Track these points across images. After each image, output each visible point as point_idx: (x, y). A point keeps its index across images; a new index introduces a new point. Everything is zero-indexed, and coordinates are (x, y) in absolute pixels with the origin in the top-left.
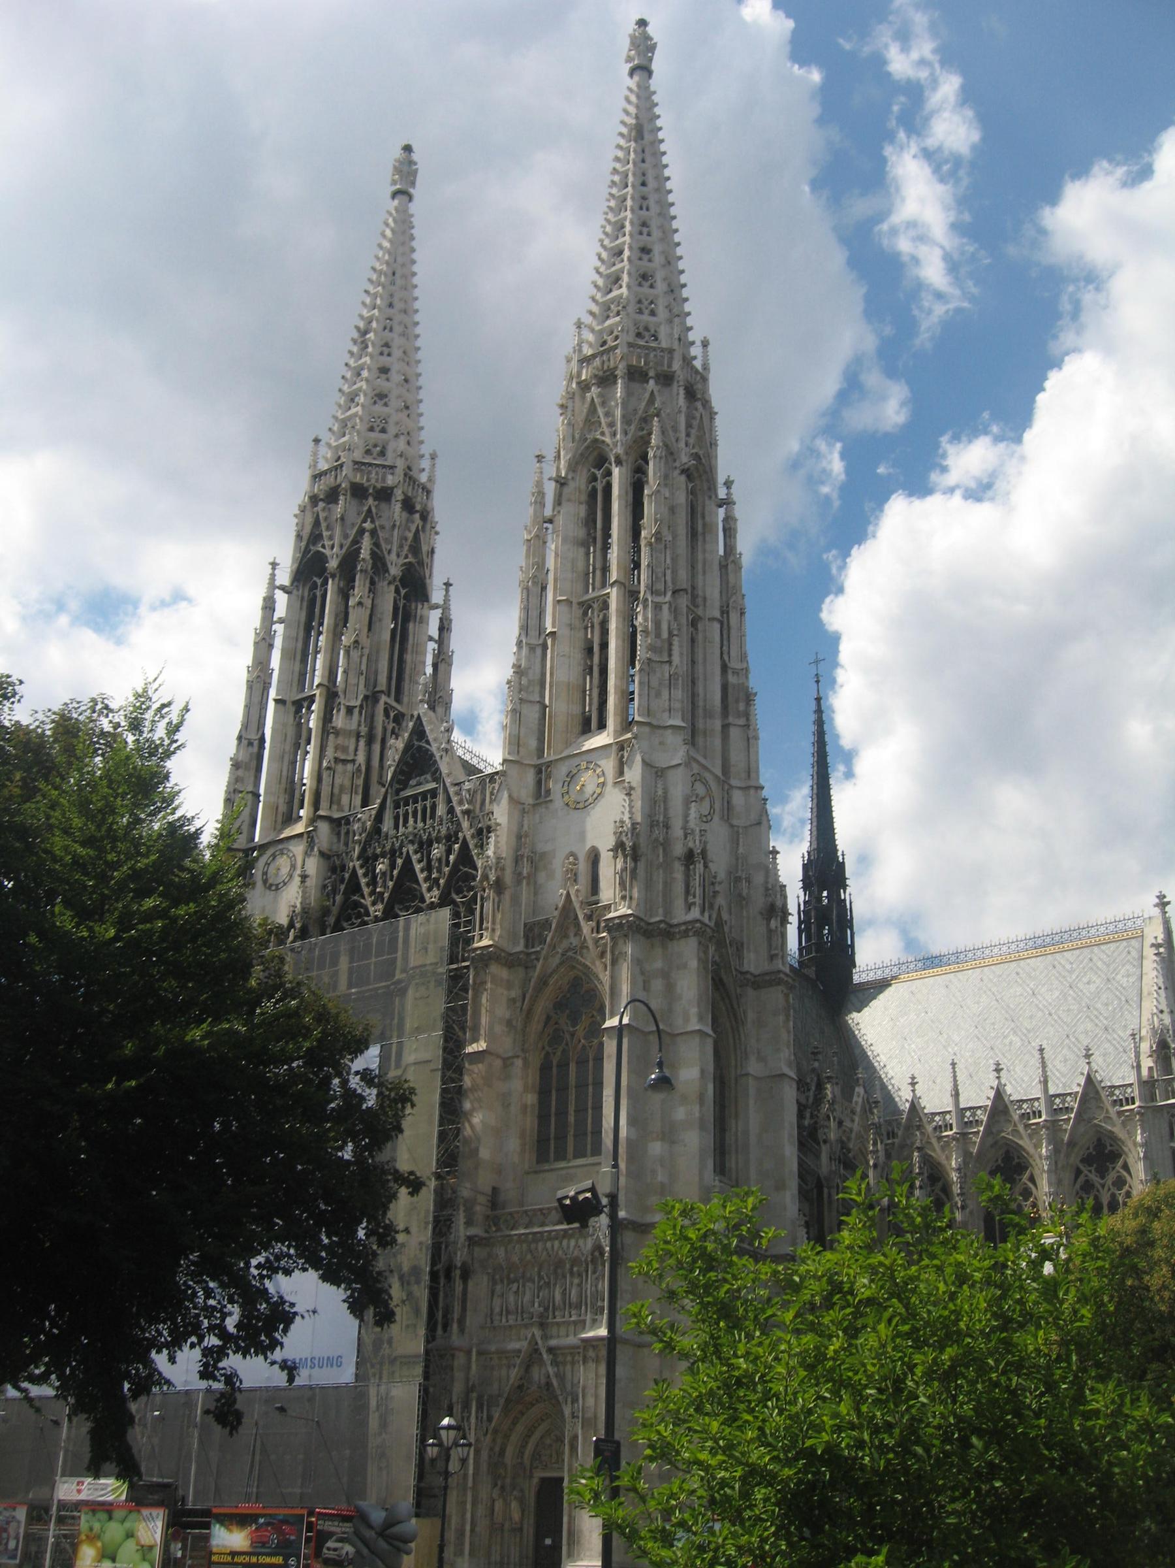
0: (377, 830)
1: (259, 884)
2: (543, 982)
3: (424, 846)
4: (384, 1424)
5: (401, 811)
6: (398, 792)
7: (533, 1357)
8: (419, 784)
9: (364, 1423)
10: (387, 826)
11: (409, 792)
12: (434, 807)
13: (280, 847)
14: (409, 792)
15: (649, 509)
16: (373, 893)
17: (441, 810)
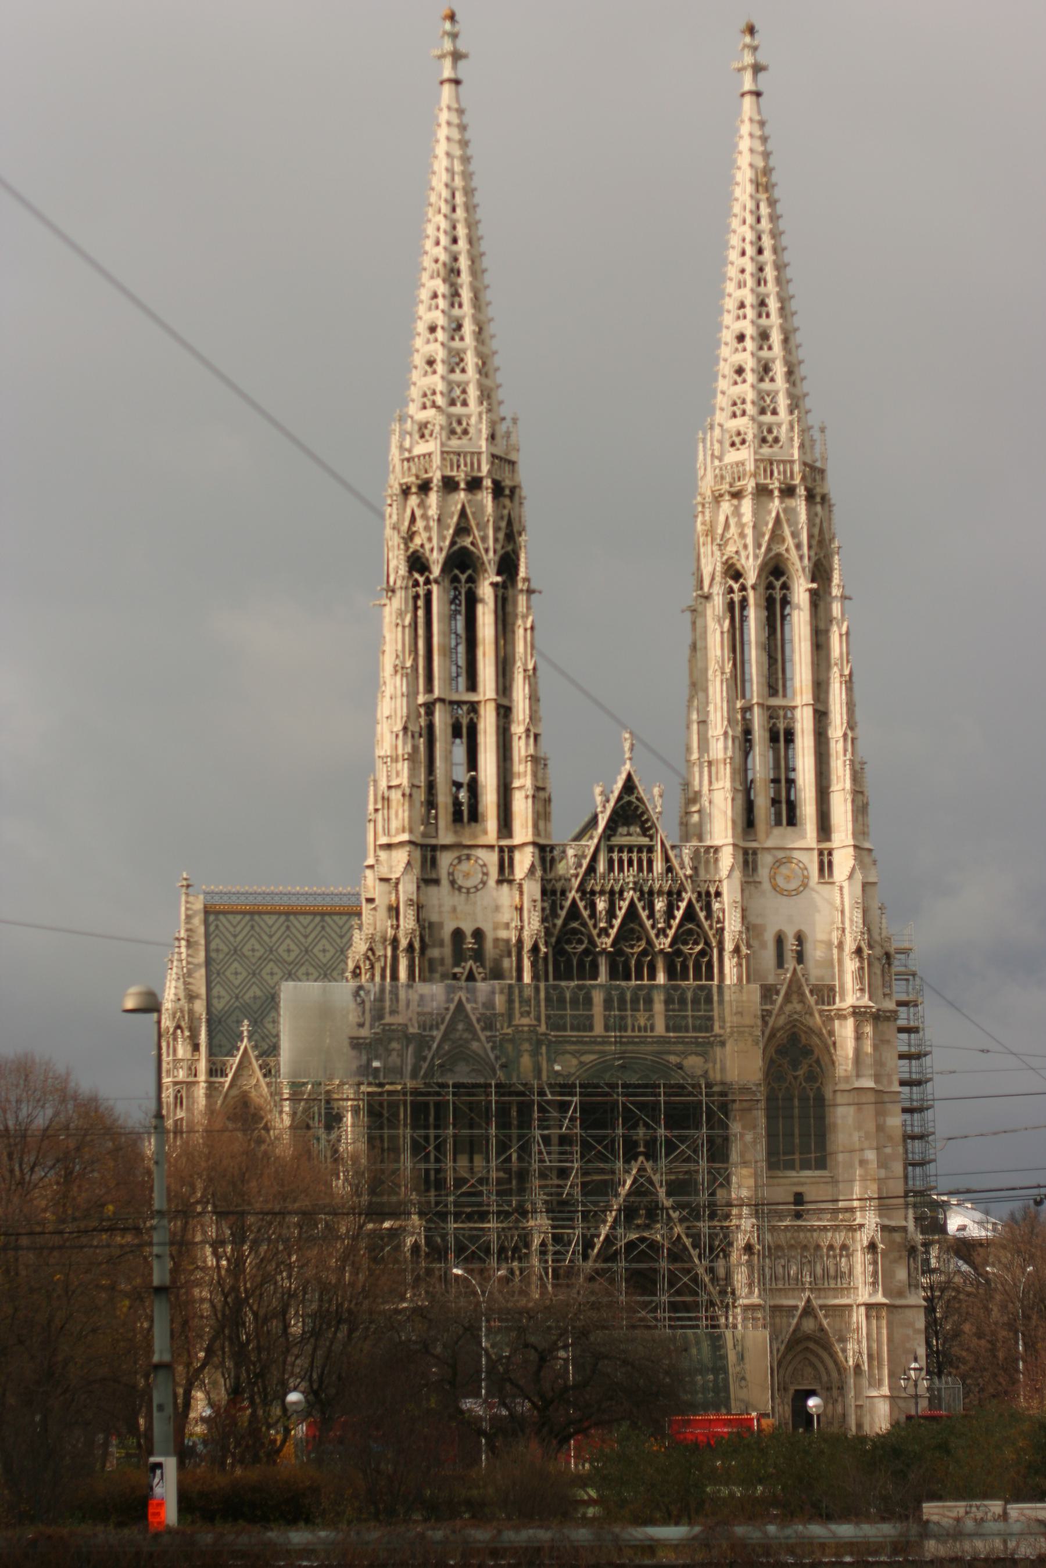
0: (591, 869)
1: (445, 882)
2: (772, 1035)
3: (648, 897)
4: (741, 1358)
5: (615, 856)
6: (609, 838)
7: (808, 1311)
8: (629, 834)
9: (724, 1357)
10: (601, 867)
11: (617, 841)
12: (650, 862)
13: (466, 852)
14: (617, 841)
15: (836, 646)
16: (595, 926)
17: (659, 866)
